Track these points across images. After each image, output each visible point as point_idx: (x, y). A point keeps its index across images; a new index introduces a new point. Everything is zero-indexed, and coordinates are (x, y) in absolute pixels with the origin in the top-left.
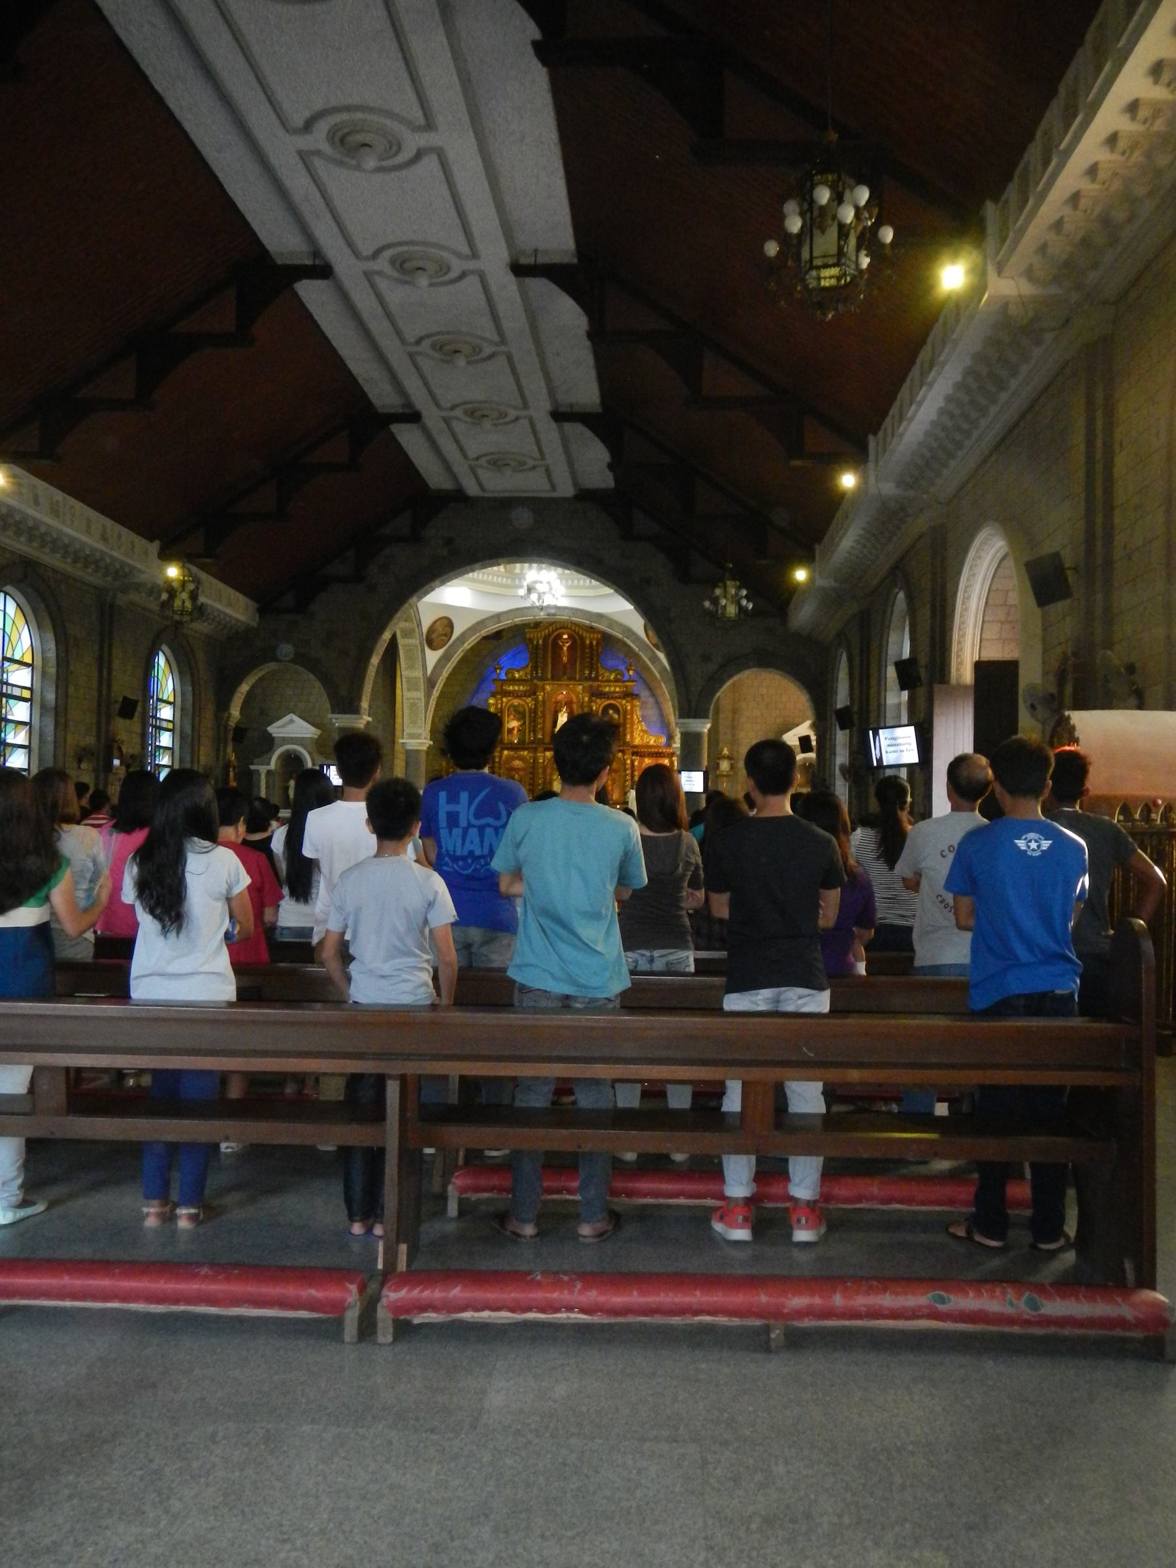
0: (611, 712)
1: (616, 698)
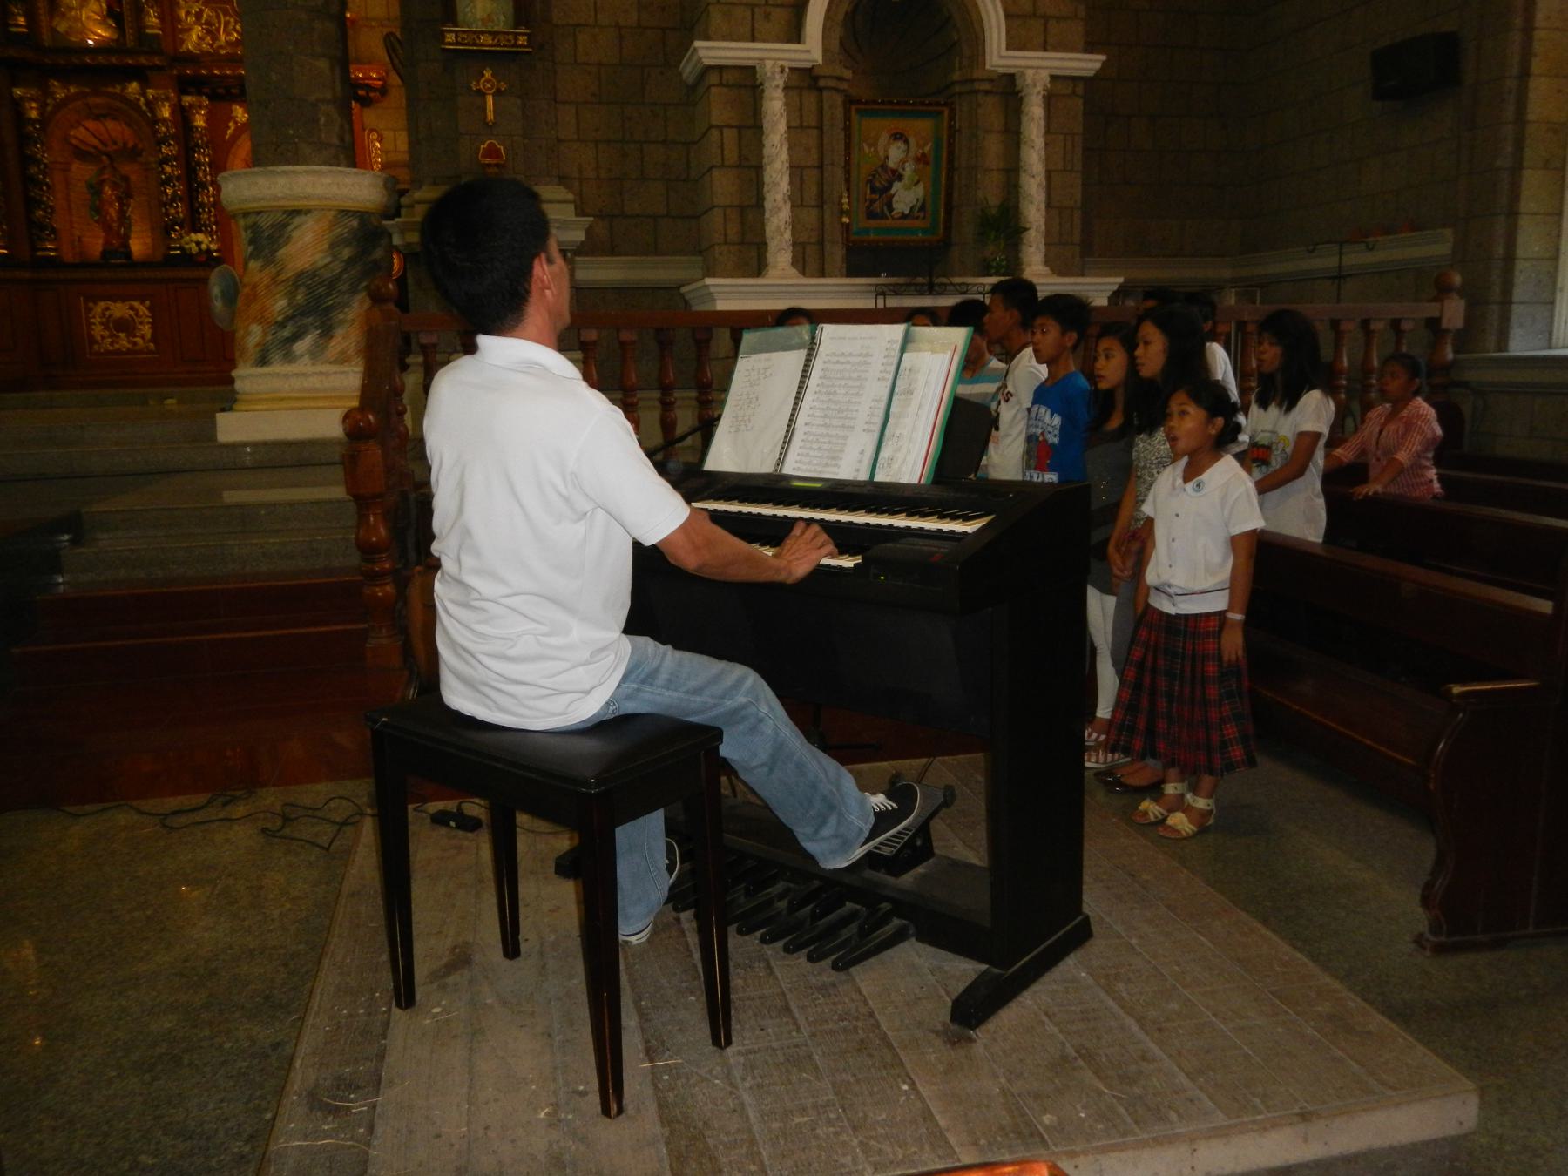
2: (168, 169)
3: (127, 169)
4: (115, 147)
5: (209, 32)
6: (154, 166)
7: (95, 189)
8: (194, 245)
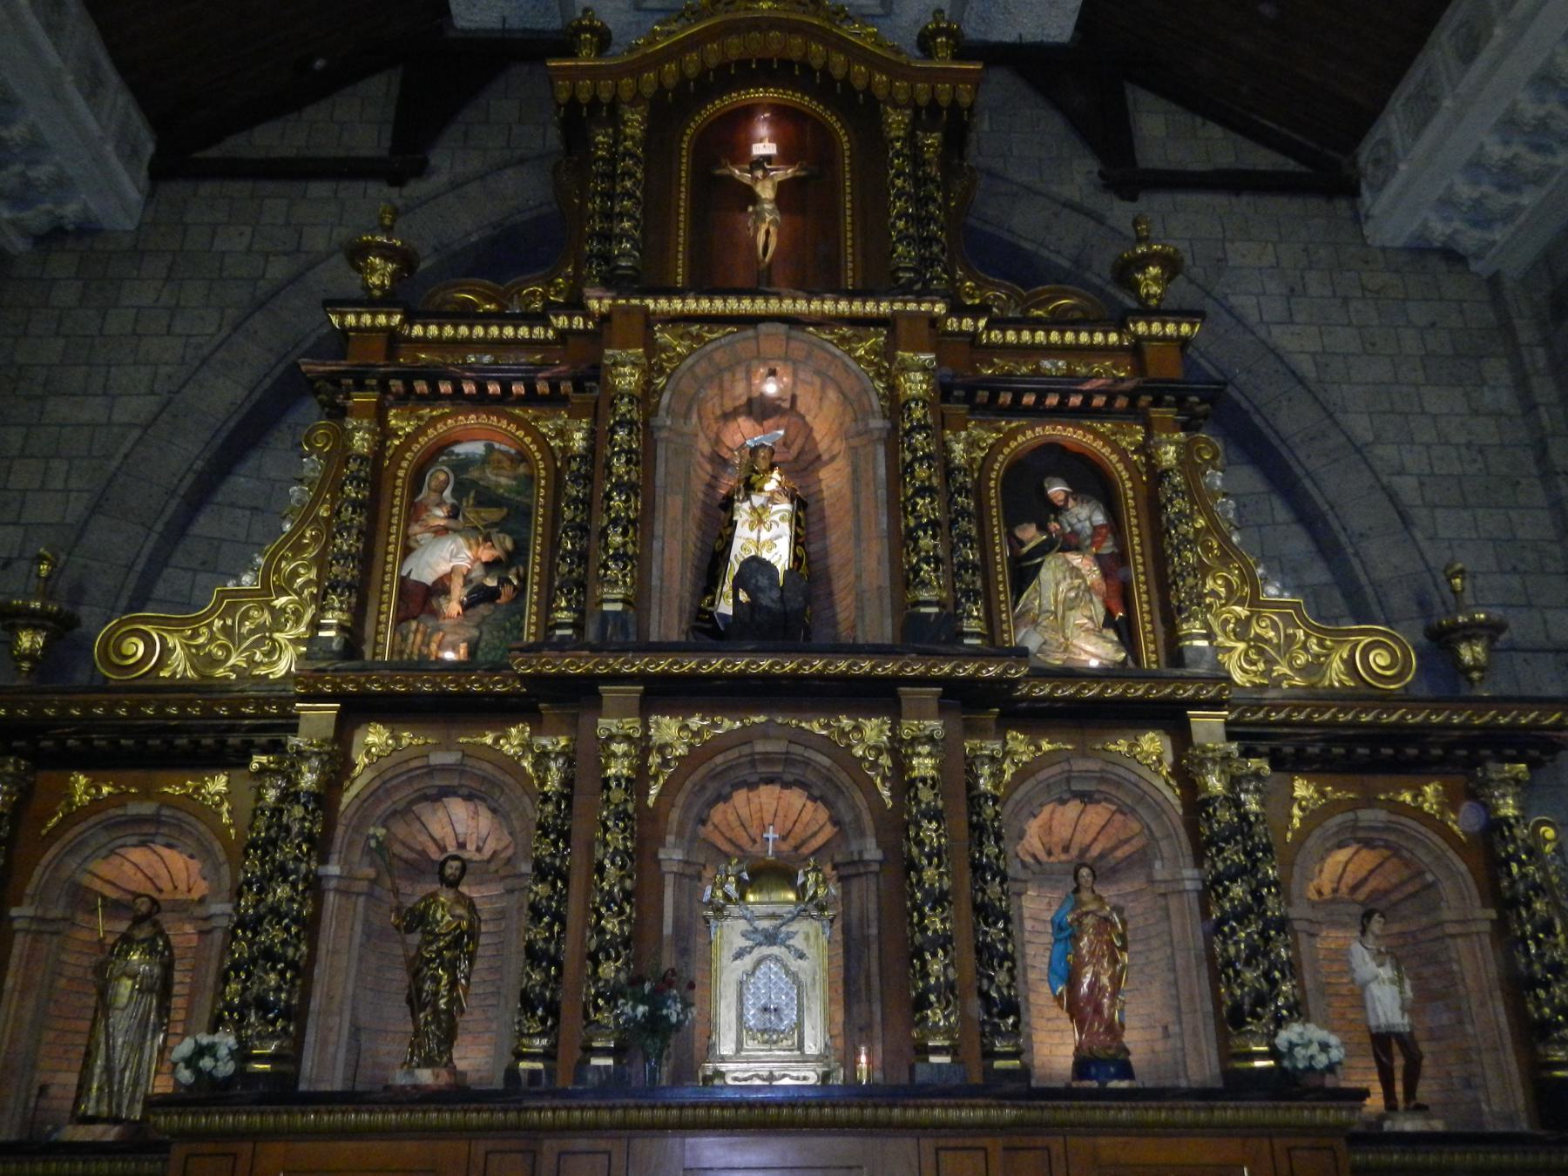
0: (1057, 490)
1: (1086, 411)
2: (1238, 890)
3: (1109, 892)
4: (1063, 857)
5: (1261, 652)
6: (1189, 885)
7: (1066, 934)
8: (1314, 1049)
